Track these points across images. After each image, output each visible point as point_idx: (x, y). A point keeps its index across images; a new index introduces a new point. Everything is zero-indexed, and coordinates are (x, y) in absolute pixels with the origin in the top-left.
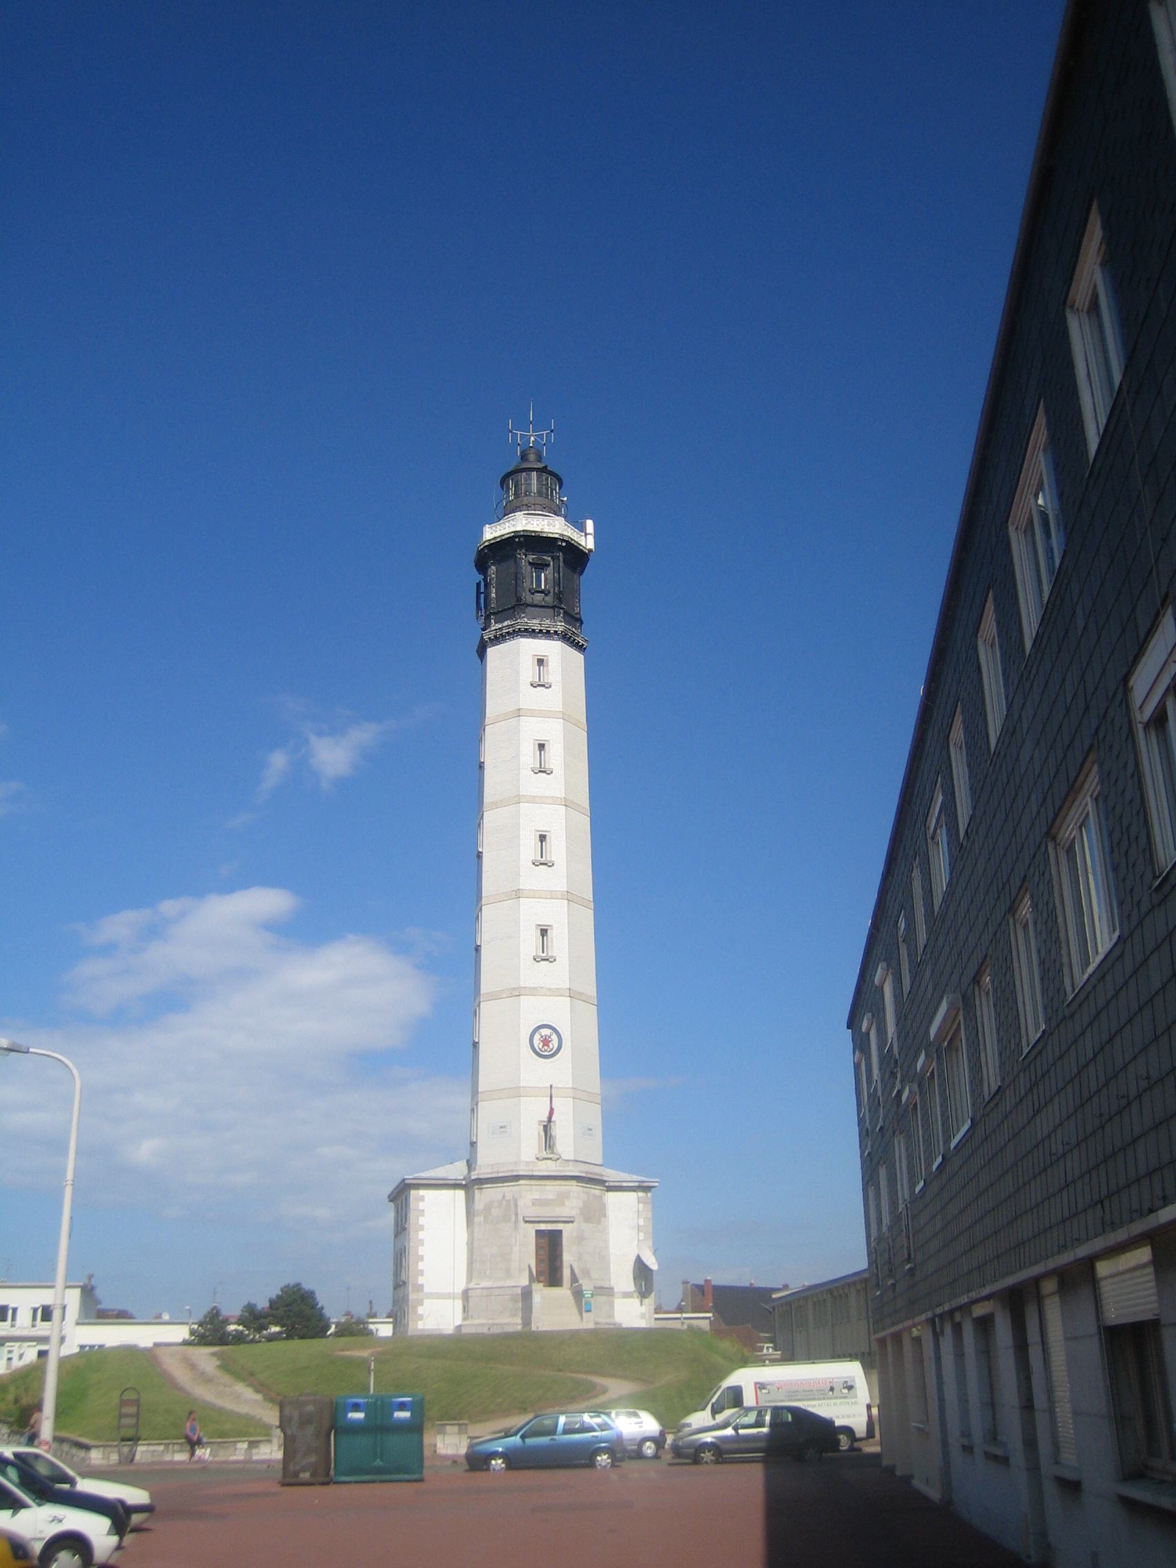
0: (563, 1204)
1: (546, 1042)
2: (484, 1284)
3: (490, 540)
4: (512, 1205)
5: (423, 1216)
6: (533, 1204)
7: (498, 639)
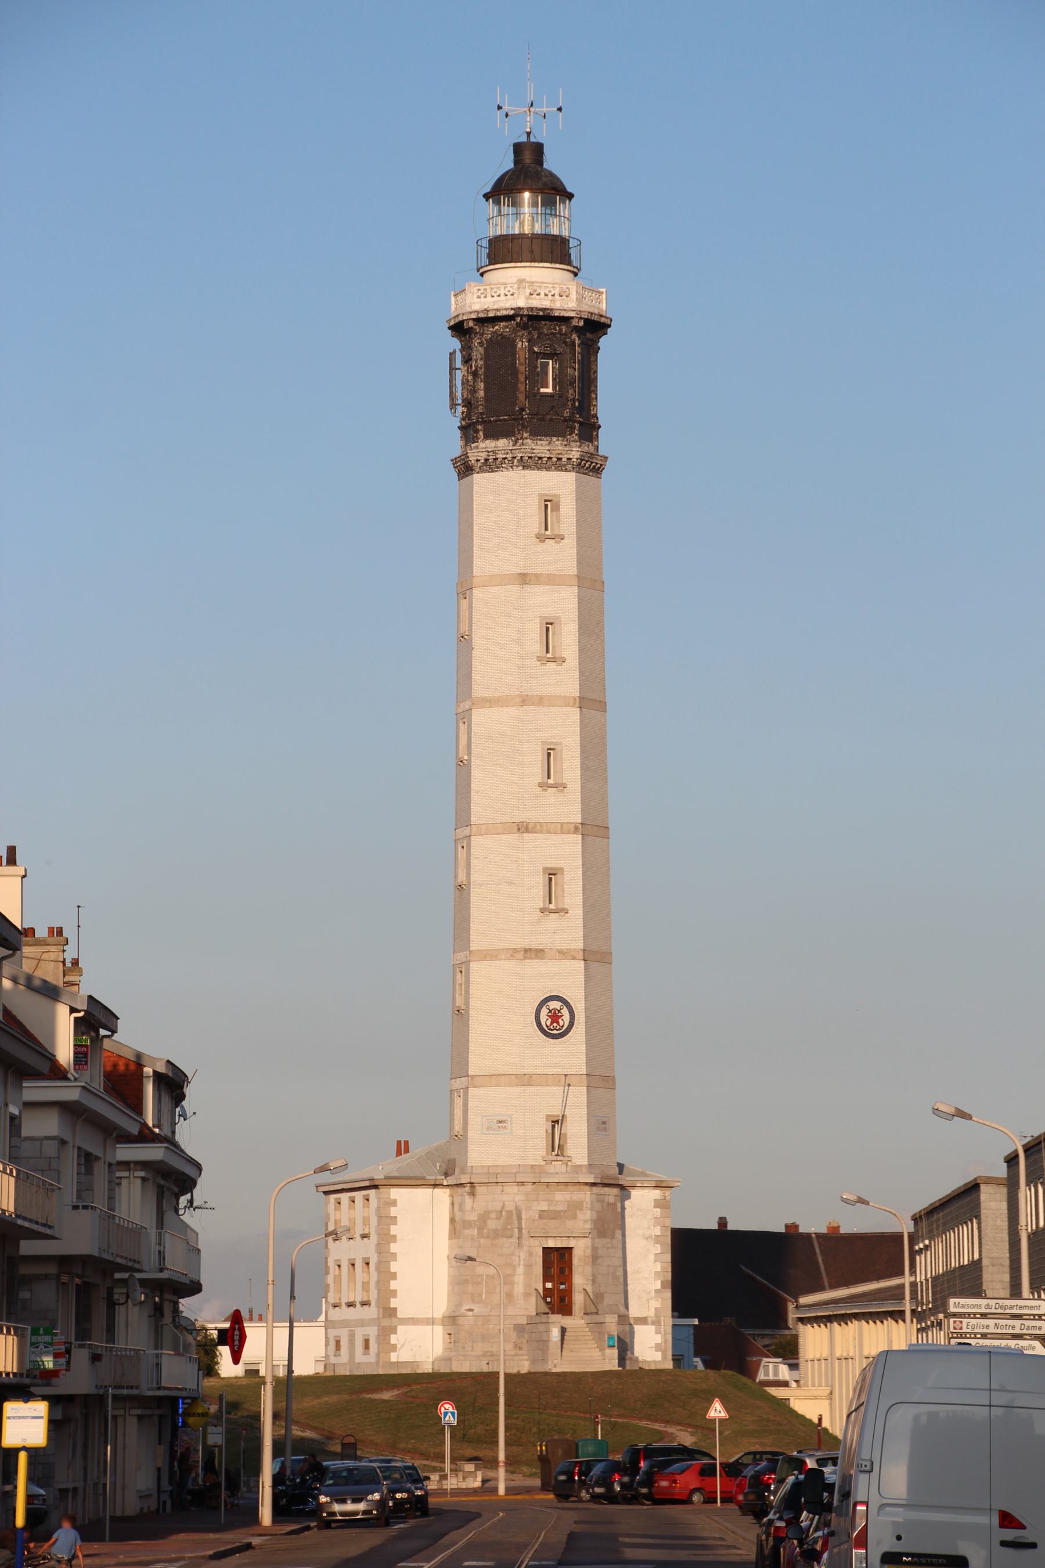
1: (555, 1017)
5: (396, 1224)
6: (540, 1217)
7: (491, 465)
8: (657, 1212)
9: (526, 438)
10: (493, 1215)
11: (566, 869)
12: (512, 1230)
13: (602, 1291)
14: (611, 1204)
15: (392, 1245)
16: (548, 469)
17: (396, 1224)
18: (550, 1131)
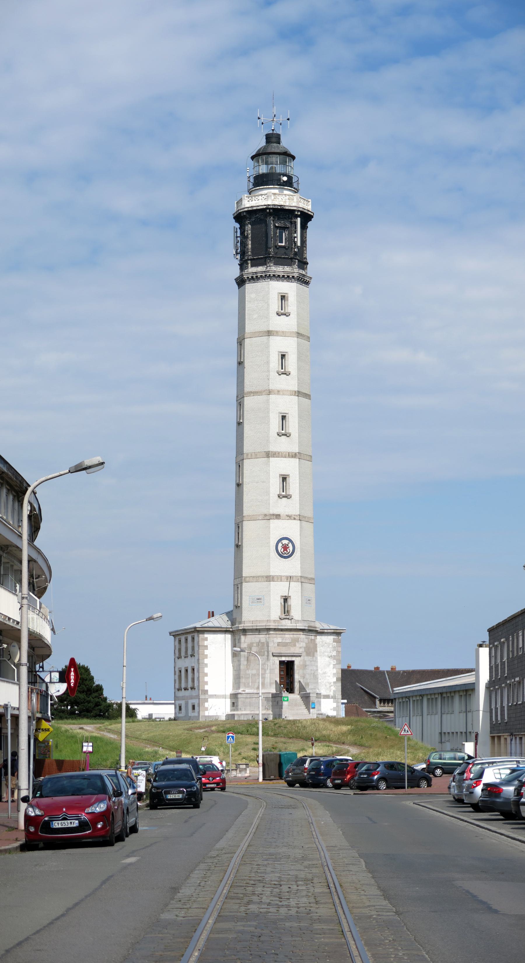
0: (295, 645)
1: (285, 547)
2: (247, 691)
3: (248, 208)
4: (265, 645)
5: (207, 649)
6: (278, 645)
7: (255, 279)
8: (334, 644)
9: (272, 266)
10: (255, 645)
11: (291, 475)
12: (264, 652)
13: (308, 682)
14: (313, 640)
15: (205, 660)
16: (283, 281)
17: (207, 649)
18: (283, 604)
